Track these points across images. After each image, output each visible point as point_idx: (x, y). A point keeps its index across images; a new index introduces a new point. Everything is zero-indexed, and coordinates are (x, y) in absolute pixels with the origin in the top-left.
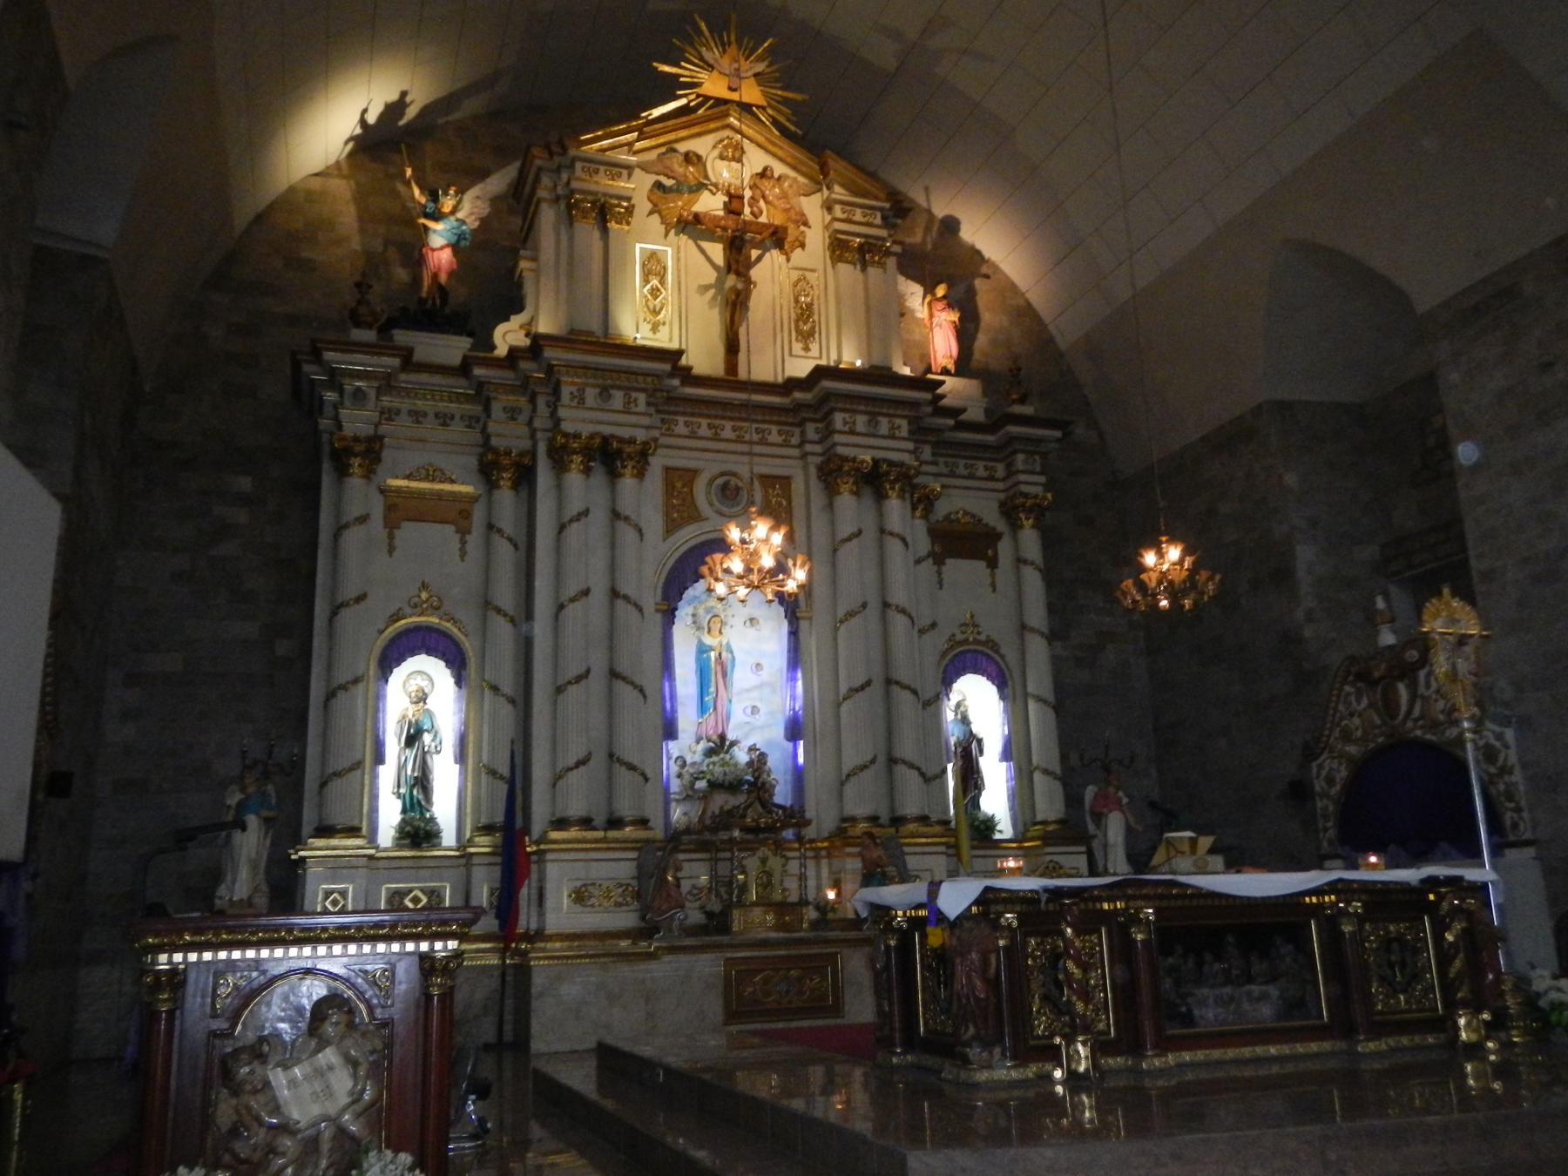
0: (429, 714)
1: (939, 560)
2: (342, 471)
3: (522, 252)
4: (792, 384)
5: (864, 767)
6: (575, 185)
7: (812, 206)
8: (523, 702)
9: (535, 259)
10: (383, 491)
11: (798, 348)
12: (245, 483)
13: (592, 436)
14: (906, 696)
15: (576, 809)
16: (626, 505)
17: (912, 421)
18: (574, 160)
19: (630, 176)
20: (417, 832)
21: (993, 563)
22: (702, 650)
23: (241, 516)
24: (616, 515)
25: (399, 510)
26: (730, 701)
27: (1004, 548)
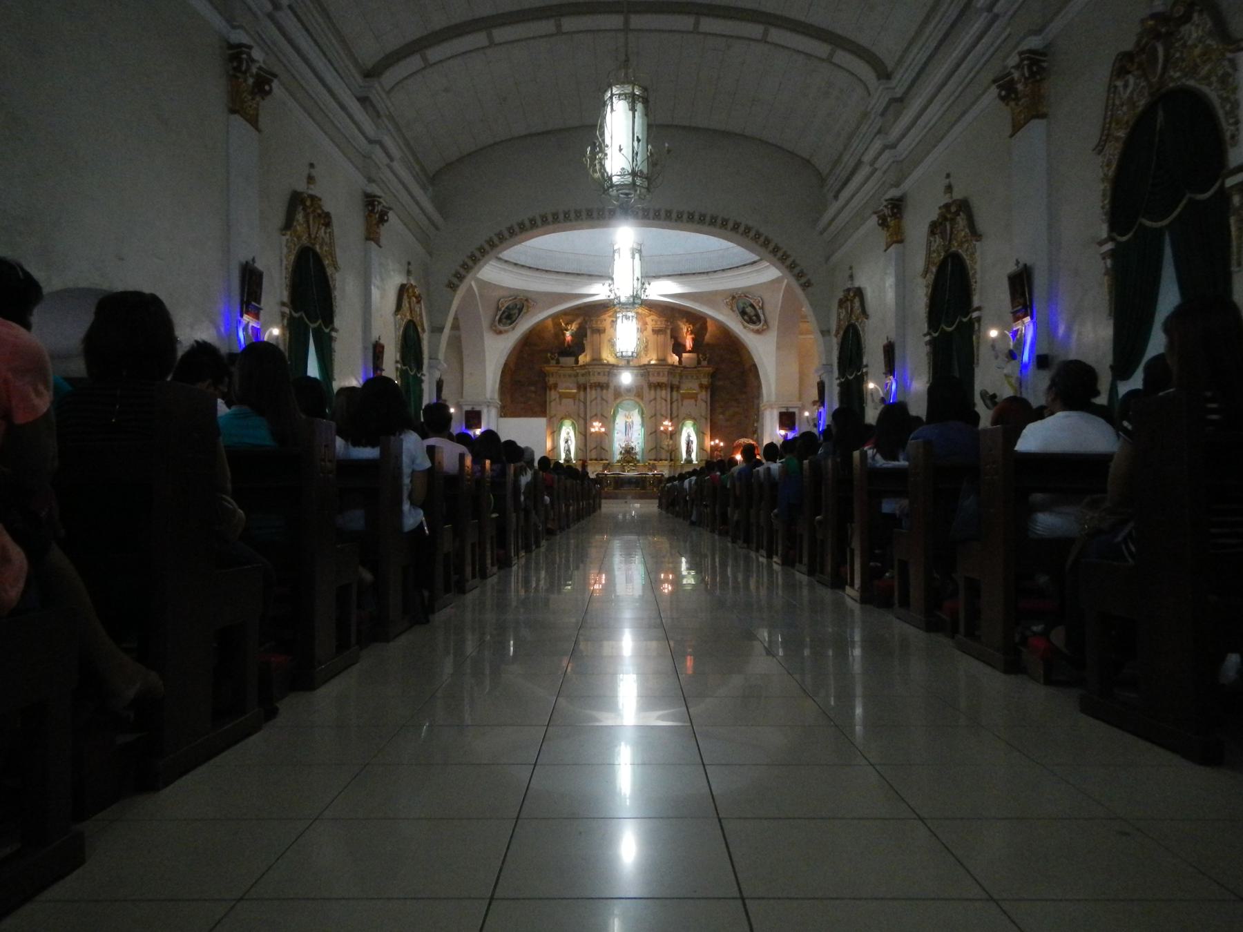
0: (570, 437)
1: (682, 401)
2: (550, 390)
3: (585, 339)
4: (640, 366)
5: (652, 449)
6: (594, 326)
7: (649, 320)
8: (585, 436)
9: (586, 340)
10: (559, 393)
11: (644, 356)
12: (533, 388)
13: (595, 383)
14: (664, 436)
15: (594, 457)
16: (604, 397)
17: (668, 372)
18: (592, 320)
19: (605, 320)
20: (568, 460)
21: (696, 401)
22: (626, 422)
23: (533, 395)
24: (603, 399)
25: (562, 396)
26: (632, 434)
27: (699, 397)
